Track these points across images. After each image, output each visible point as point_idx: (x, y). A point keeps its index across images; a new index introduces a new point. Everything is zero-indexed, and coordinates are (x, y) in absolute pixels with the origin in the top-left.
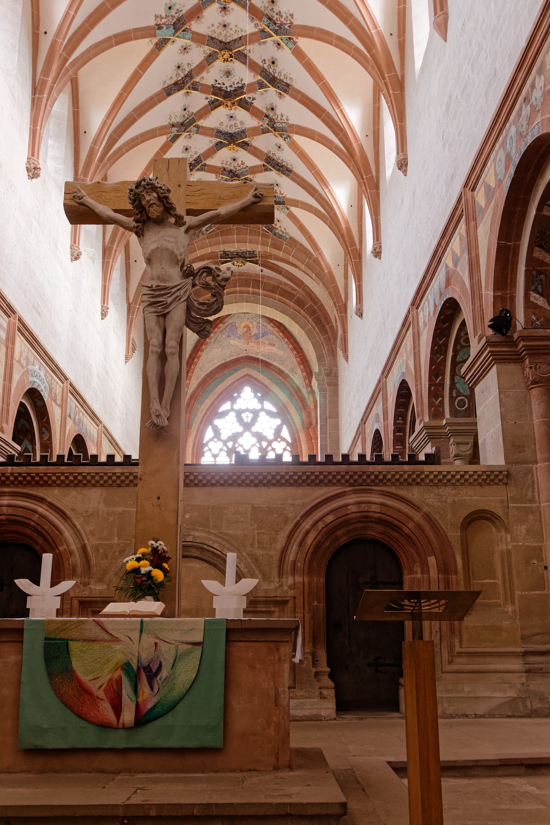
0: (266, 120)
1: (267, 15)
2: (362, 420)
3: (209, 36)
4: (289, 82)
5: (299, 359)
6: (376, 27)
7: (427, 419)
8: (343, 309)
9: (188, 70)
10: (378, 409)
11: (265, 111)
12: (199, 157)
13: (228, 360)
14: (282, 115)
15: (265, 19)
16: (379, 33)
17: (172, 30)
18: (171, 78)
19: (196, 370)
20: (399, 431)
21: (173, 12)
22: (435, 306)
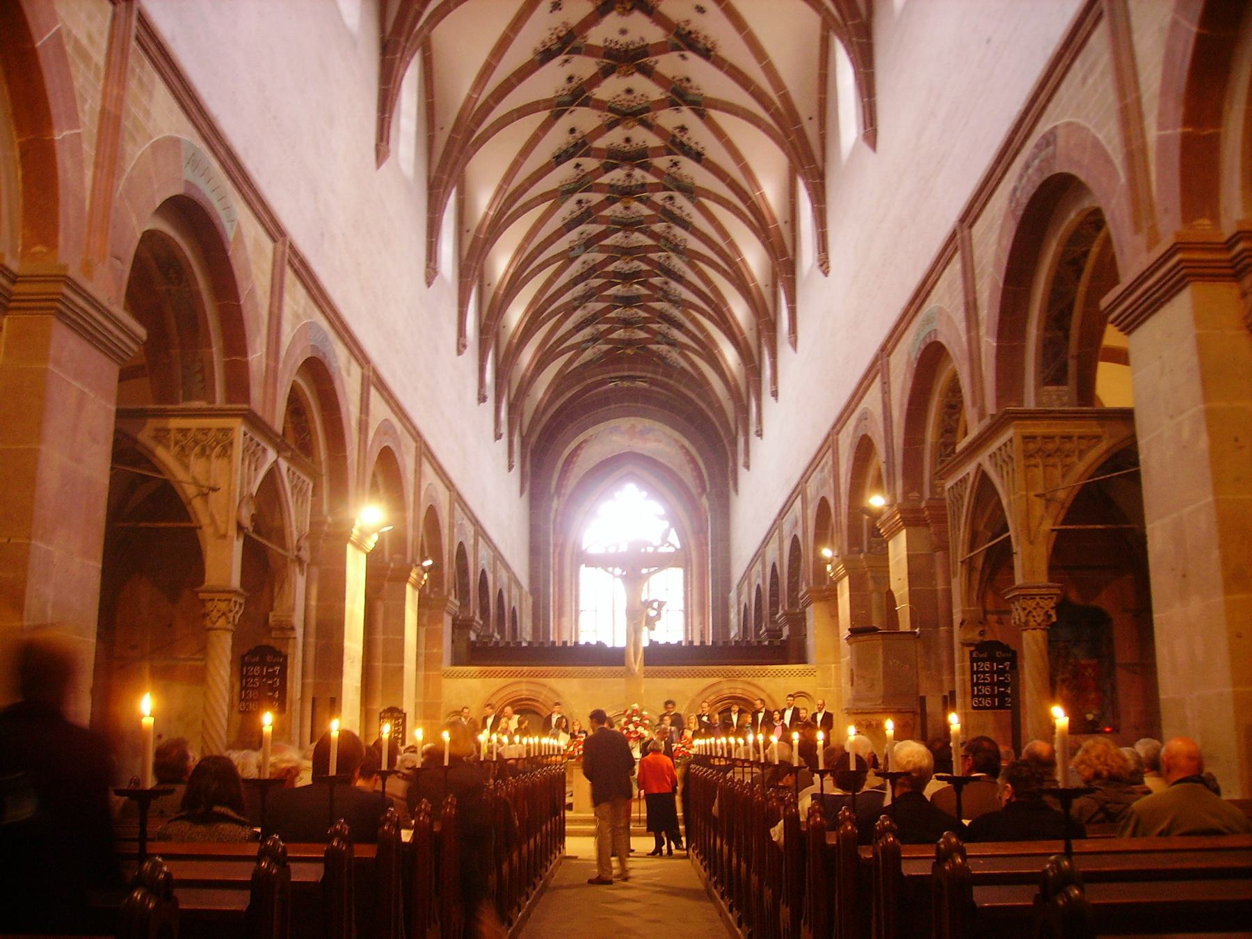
0: (661, 293)
1: (664, 237)
2: (748, 567)
3: (612, 245)
4: (681, 273)
5: (688, 458)
6: (753, 280)
7: (786, 608)
8: (734, 443)
9: (592, 264)
10: (758, 566)
11: (659, 285)
12: (595, 313)
13: (609, 456)
14: (675, 290)
15: (662, 240)
16: (757, 287)
17: (582, 248)
18: (577, 271)
19: (575, 469)
20: (775, 596)
21: (584, 236)
22: (791, 532)
